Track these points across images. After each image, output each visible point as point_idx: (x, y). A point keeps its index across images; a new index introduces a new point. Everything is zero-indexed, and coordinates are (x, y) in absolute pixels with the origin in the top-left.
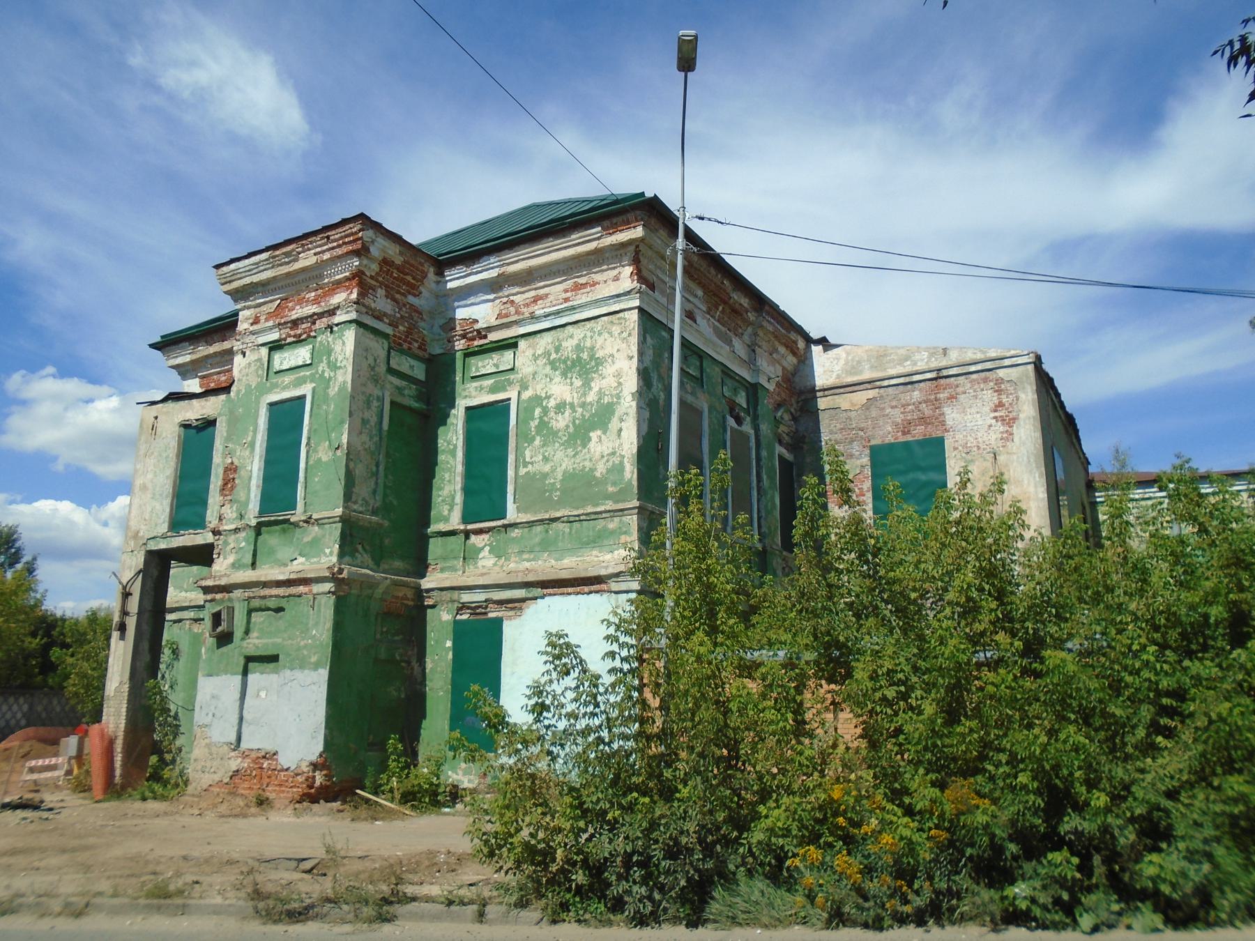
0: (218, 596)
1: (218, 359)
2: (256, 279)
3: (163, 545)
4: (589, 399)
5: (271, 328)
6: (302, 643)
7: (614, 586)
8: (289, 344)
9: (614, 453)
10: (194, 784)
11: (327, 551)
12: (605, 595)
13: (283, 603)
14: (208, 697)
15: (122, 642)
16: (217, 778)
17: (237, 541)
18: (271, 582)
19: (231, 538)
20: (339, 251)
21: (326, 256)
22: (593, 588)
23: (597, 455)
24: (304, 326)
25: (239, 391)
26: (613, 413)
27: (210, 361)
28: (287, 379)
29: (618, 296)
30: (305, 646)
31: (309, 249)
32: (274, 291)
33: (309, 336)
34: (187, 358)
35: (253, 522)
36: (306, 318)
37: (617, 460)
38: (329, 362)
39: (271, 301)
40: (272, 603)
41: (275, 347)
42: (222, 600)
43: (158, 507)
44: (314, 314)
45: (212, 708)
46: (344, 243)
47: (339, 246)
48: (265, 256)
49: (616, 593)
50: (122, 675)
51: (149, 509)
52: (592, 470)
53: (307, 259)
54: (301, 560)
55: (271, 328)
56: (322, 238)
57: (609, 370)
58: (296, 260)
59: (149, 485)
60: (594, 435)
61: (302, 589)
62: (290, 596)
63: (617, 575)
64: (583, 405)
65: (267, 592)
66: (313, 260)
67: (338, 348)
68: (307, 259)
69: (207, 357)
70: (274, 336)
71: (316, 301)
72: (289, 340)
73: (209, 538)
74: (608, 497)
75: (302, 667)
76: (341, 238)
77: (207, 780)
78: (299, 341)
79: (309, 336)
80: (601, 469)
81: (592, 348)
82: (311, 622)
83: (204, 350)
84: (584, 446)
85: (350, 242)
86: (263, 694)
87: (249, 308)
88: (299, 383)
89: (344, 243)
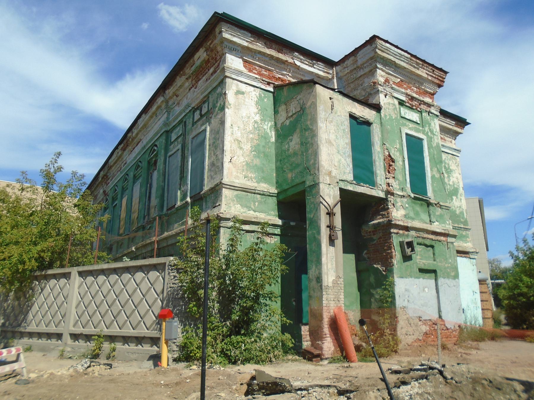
0: (401, 232)
1: (267, 59)
2: (397, 61)
3: (350, 188)
4: (451, 183)
5: (402, 93)
6: (446, 265)
7: (471, 256)
8: (407, 106)
9: (460, 207)
10: (403, 343)
11: (448, 222)
12: (468, 259)
13: (433, 243)
14: (404, 290)
15: (331, 247)
16: (415, 337)
17: (402, 202)
18: (430, 231)
19: (398, 200)
20: (433, 79)
21: (430, 78)
22: (466, 255)
23: (456, 206)
24: (416, 103)
25: (385, 116)
26: (458, 192)
27: (259, 56)
28: (411, 125)
29: (455, 150)
30: (448, 267)
31: (424, 69)
32: (400, 74)
33: (416, 109)
34: (246, 44)
35: (412, 195)
36: (419, 100)
37: (461, 210)
38: (430, 130)
39: (396, 77)
40: (428, 242)
41: (401, 103)
42: (403, 234)
43: (343, 160)
44: (423, 101)
45: (407, 296)
46: (438, 79)
47: (435, 78)
48: (409, 56)
49: (470, 258)
50: (337, 271)
51: (337, 160)
52: (455, 211)
53: (422, 72)
54: (436, 223)
55: (402, 93)
56: (431, 69)
57: (455, 175)
58: (418, 69)
59: (334, 143)
60: (454, 198)
61: (442, 238)
62: (437, 240)
63: (473, 252)
64: (449, 185)
65: (426, 235)
66: (426, 76)
67: (432, 124)
68: (422, 72)
69: (260, 52)
70: (403, 98)
71: (416, 93)
72: (407, 104)
73: (382, 195)
74: (462, 222)
75: (448, 278)
76: (438, 75)
77: (410, 339)
78: (411, 108)
79: (416, 109)
80: (458, 212)
81: (448, 164)
82: (448, 256)
83: (259, 46)
84: (452, 201)
85: (440, 80)
86: (426, 290)
87: (383, 71)
88: (417, 131)
89: (438, 79)
